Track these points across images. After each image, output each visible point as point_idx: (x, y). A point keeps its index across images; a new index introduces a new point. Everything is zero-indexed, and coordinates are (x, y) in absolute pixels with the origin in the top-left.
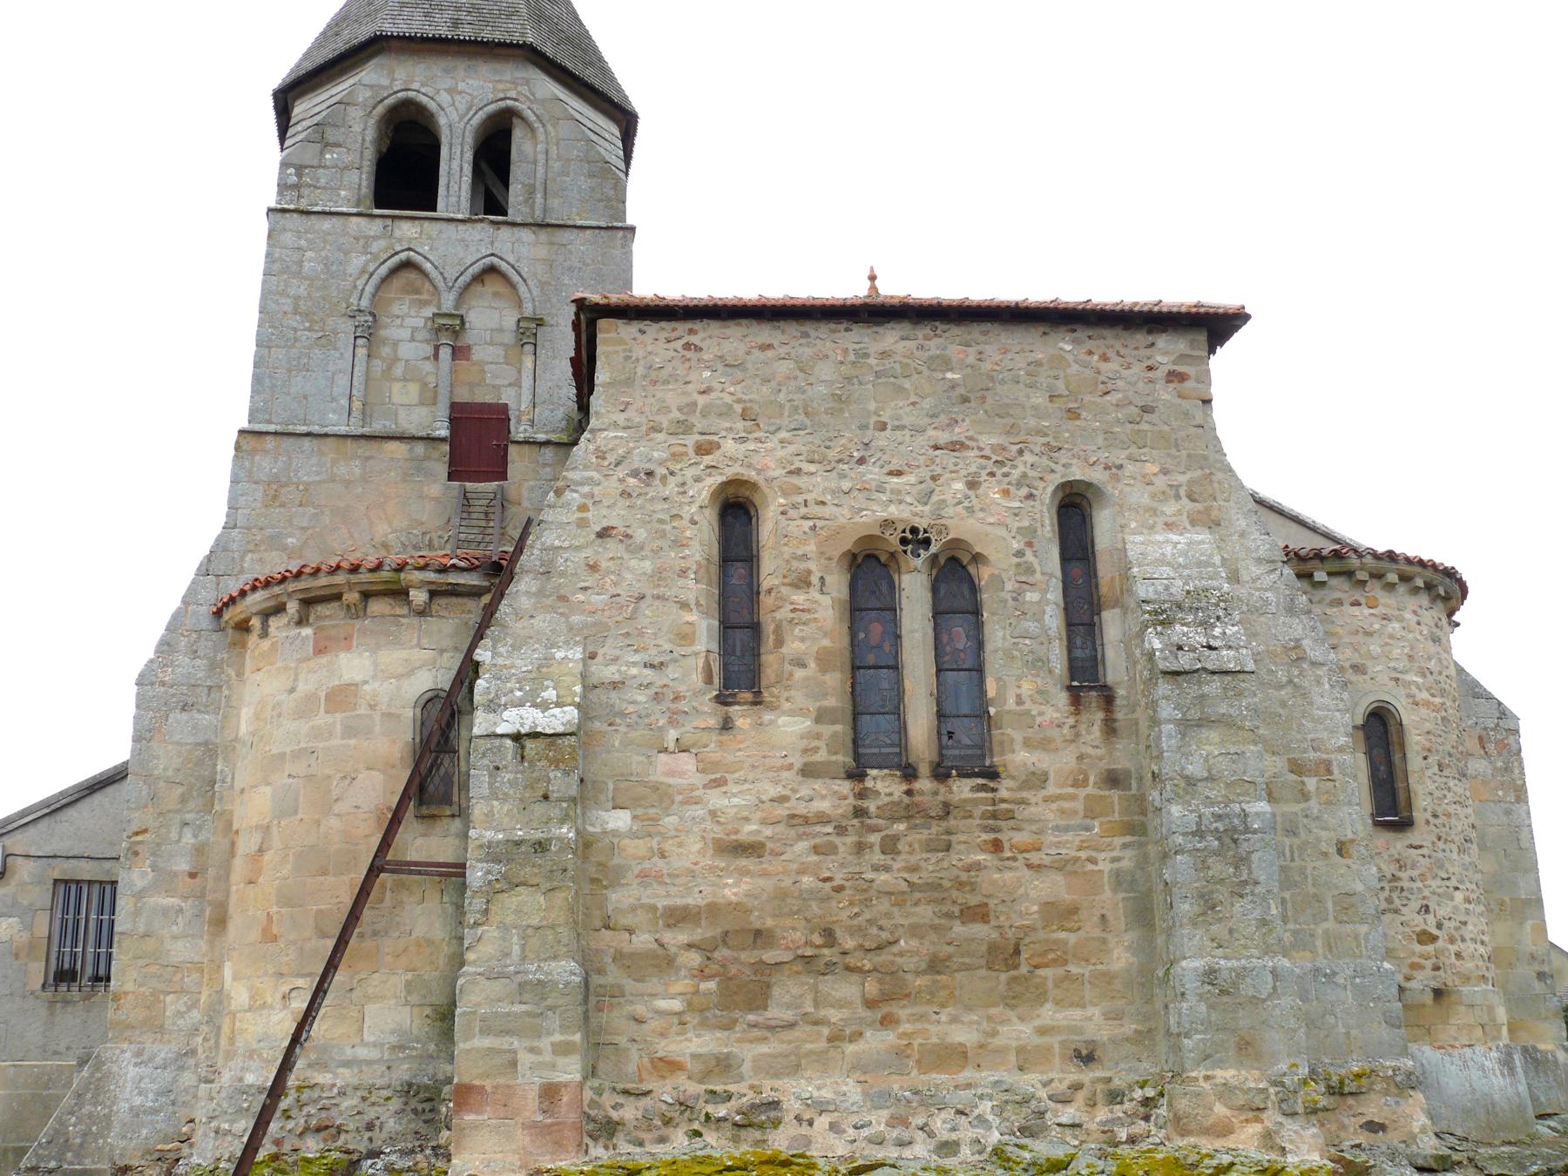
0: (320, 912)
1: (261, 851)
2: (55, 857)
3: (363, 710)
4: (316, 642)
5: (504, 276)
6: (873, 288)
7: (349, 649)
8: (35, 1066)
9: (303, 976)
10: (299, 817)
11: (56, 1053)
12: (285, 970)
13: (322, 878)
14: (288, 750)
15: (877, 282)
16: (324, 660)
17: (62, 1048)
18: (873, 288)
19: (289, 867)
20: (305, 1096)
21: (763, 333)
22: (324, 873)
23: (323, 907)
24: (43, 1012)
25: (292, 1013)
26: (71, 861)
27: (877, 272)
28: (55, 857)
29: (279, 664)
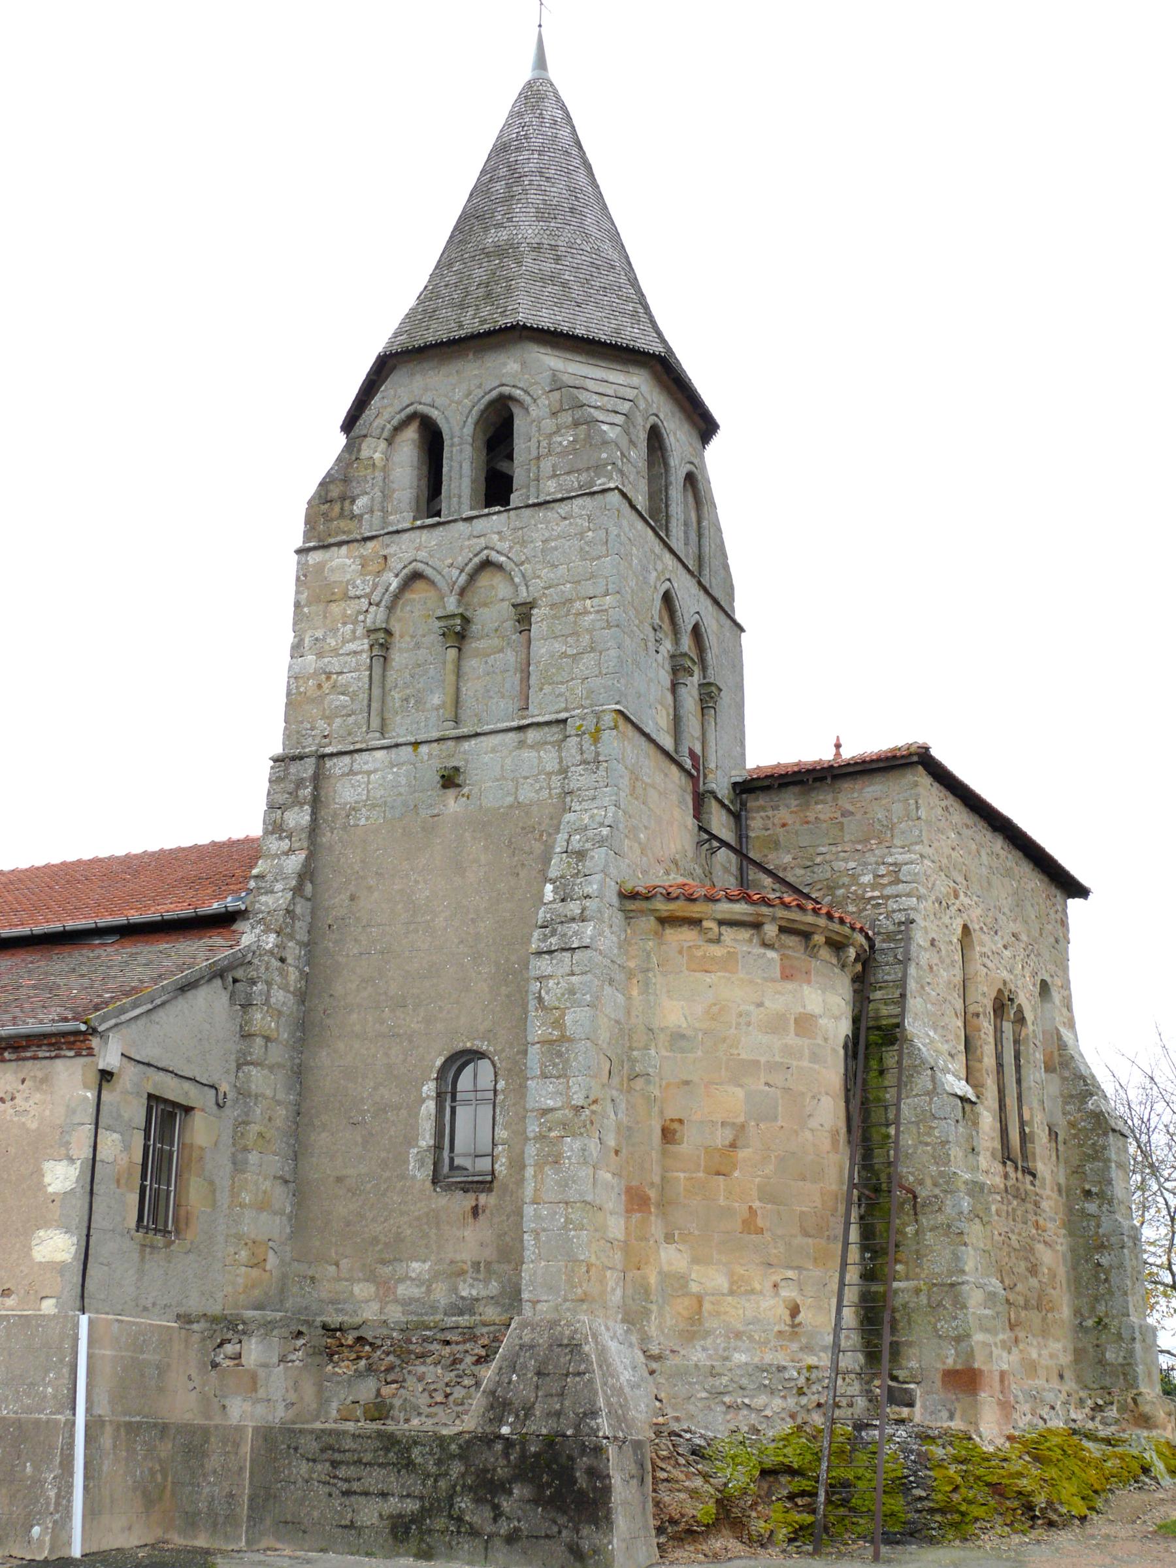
0: (802, 1213)
1: (733, 1145)
2: (149, 1065)
3: (820, 1041)
4: (783, 968)
5: (499, 567)
6: (838, 754)
7: (809, 982)
8: (134, 1323)
9: (792, 1268)
10: (780, 1123)
11: (145, 1309)
12: (774, 1261)
13: (801, 1183)
14: (763, 1060)
15: (842, 750)
16: (789, 986)
17: (149, 1304)
18: (838, 754)
19: (772, 1167)
20: (813, 1377)
21: (960, 815)
22: (804, 1179)
23: (804, 1209)
24: (136, 1256)
25: (784, 1301)
26: (161, 1073)
27: (841, 741)
28: (149, 1065)
29: (741, 975)
